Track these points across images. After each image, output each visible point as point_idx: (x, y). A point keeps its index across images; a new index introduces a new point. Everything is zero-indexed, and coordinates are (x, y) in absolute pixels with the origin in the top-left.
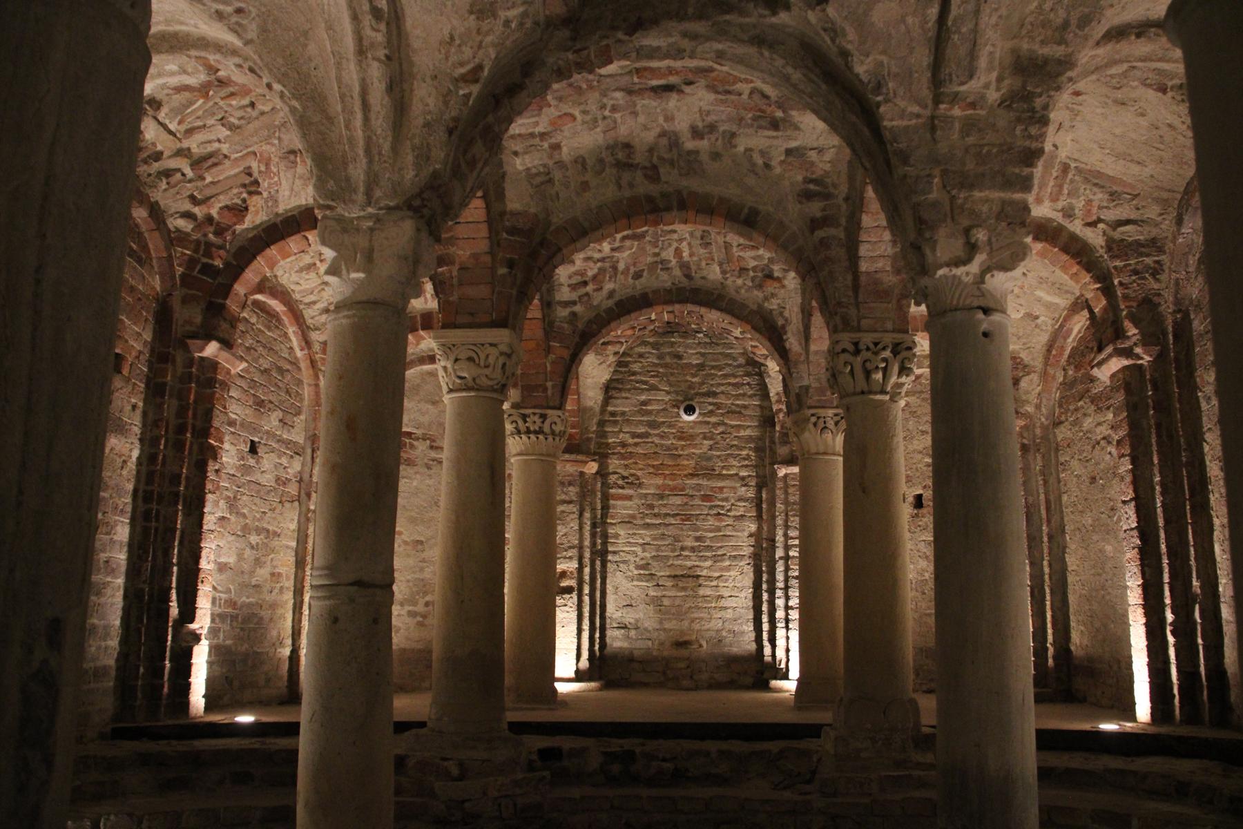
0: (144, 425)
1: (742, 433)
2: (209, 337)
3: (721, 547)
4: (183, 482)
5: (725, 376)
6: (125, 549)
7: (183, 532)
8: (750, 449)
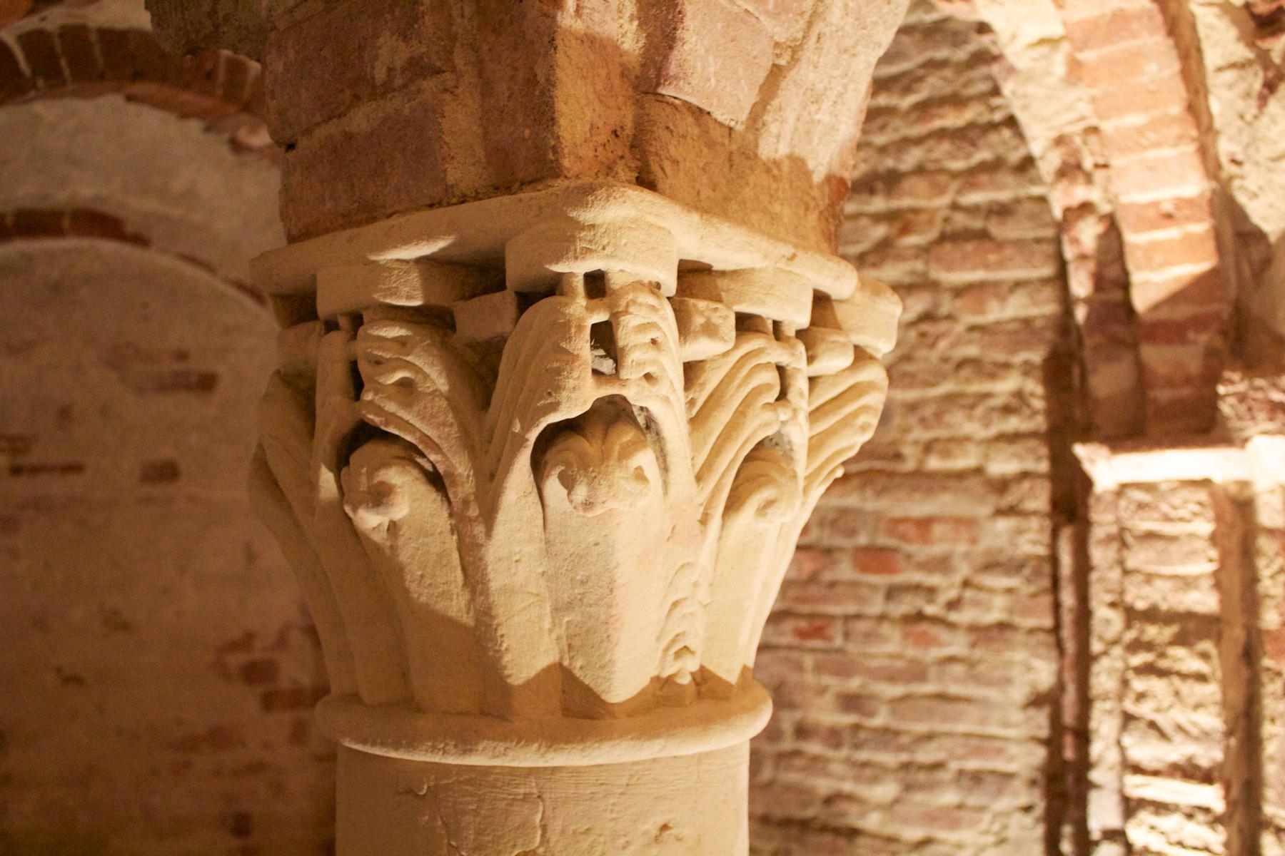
1: (998, 312)
3: (930, 737)
5: (924, 109)
8: (1027, 369)
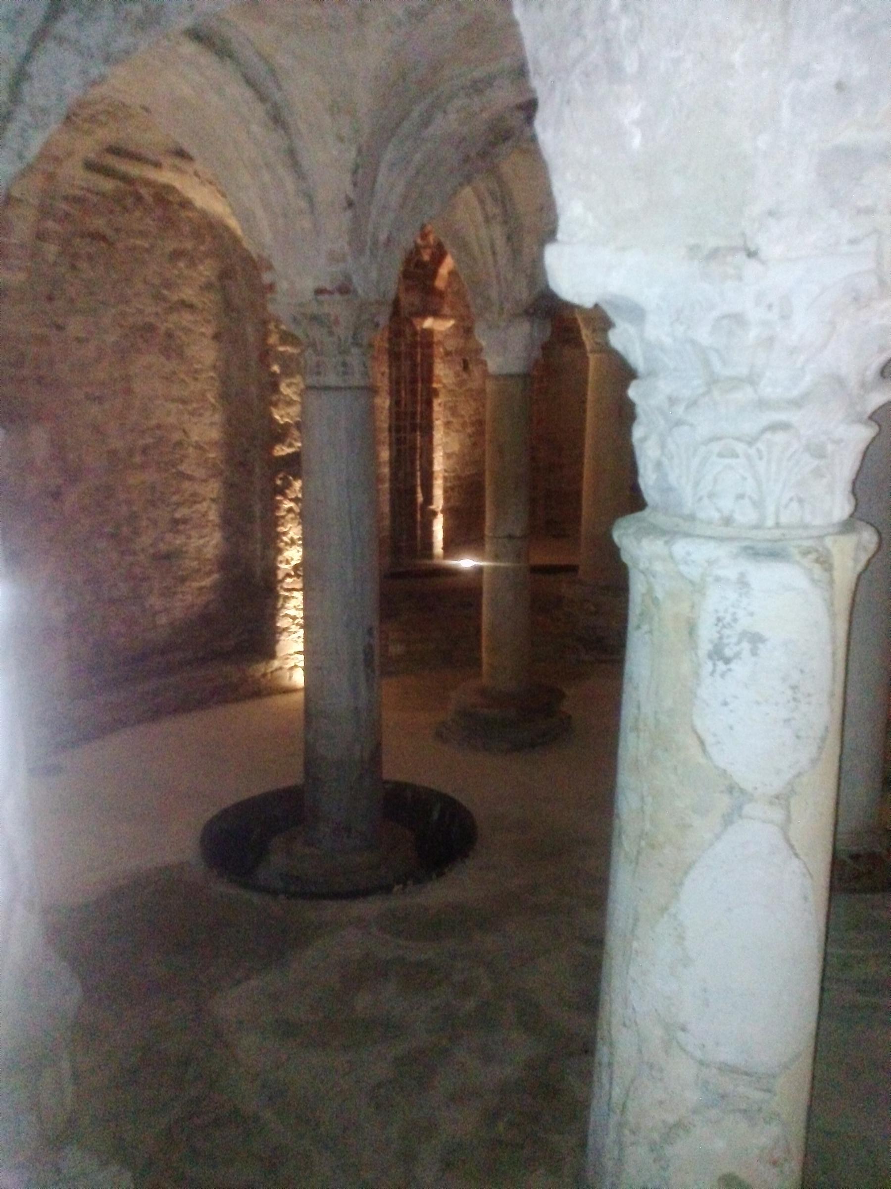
0: (391, 382)
2: (424, 314)
4: (419, 416)
6: (388, 465)
7: (421, 448)
